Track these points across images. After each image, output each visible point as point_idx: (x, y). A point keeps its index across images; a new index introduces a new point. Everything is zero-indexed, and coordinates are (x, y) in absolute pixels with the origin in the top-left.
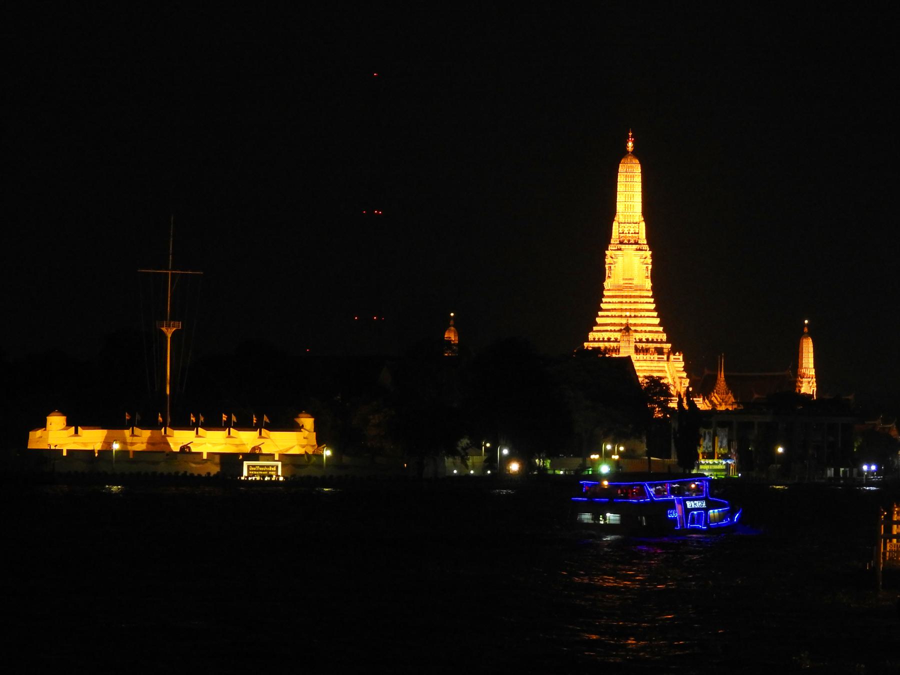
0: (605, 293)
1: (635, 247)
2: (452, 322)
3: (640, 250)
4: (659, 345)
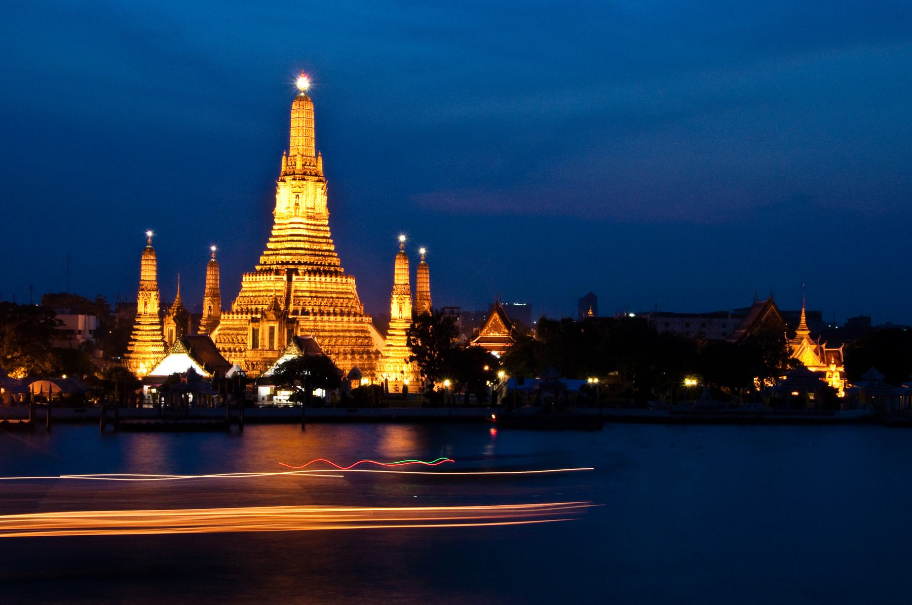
0: (276, 221)
1: (292, 177)
3: (294, 179)
4: (293, 267)
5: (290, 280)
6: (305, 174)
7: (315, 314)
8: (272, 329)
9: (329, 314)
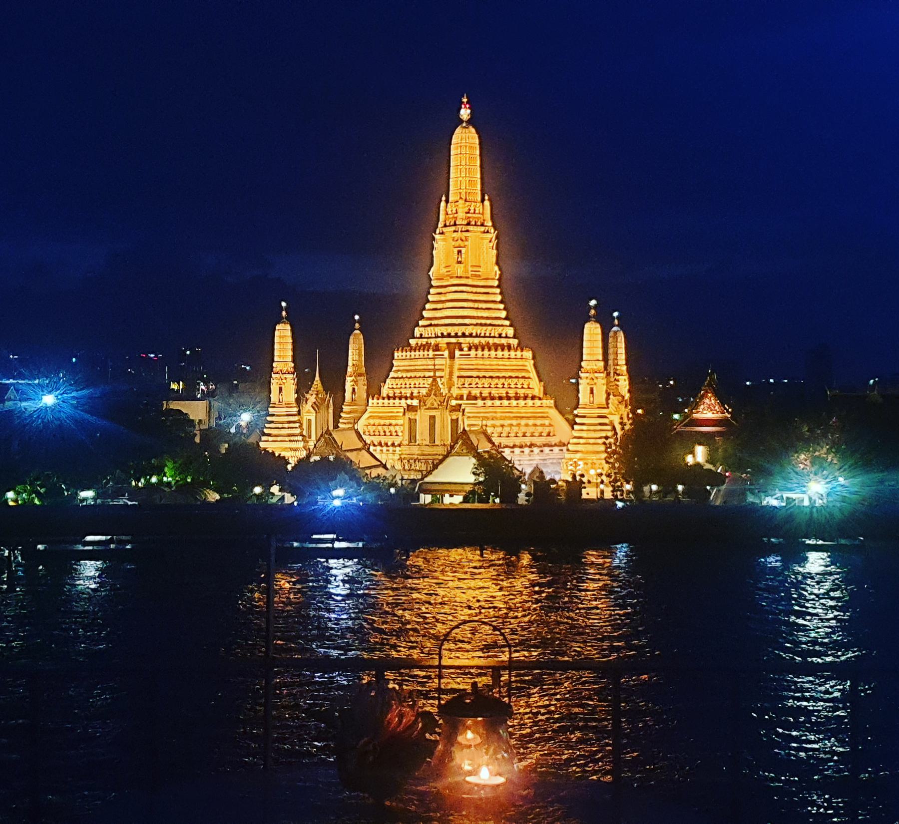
0: (434, 283)
1: (453, 228)
2: (357, 325)
3: (455, 231)
4: (453, 340)
5: (452, 356)
6: (468, 224)
7: (484, 399)
8: (432, 418)
9: (501, 398)
